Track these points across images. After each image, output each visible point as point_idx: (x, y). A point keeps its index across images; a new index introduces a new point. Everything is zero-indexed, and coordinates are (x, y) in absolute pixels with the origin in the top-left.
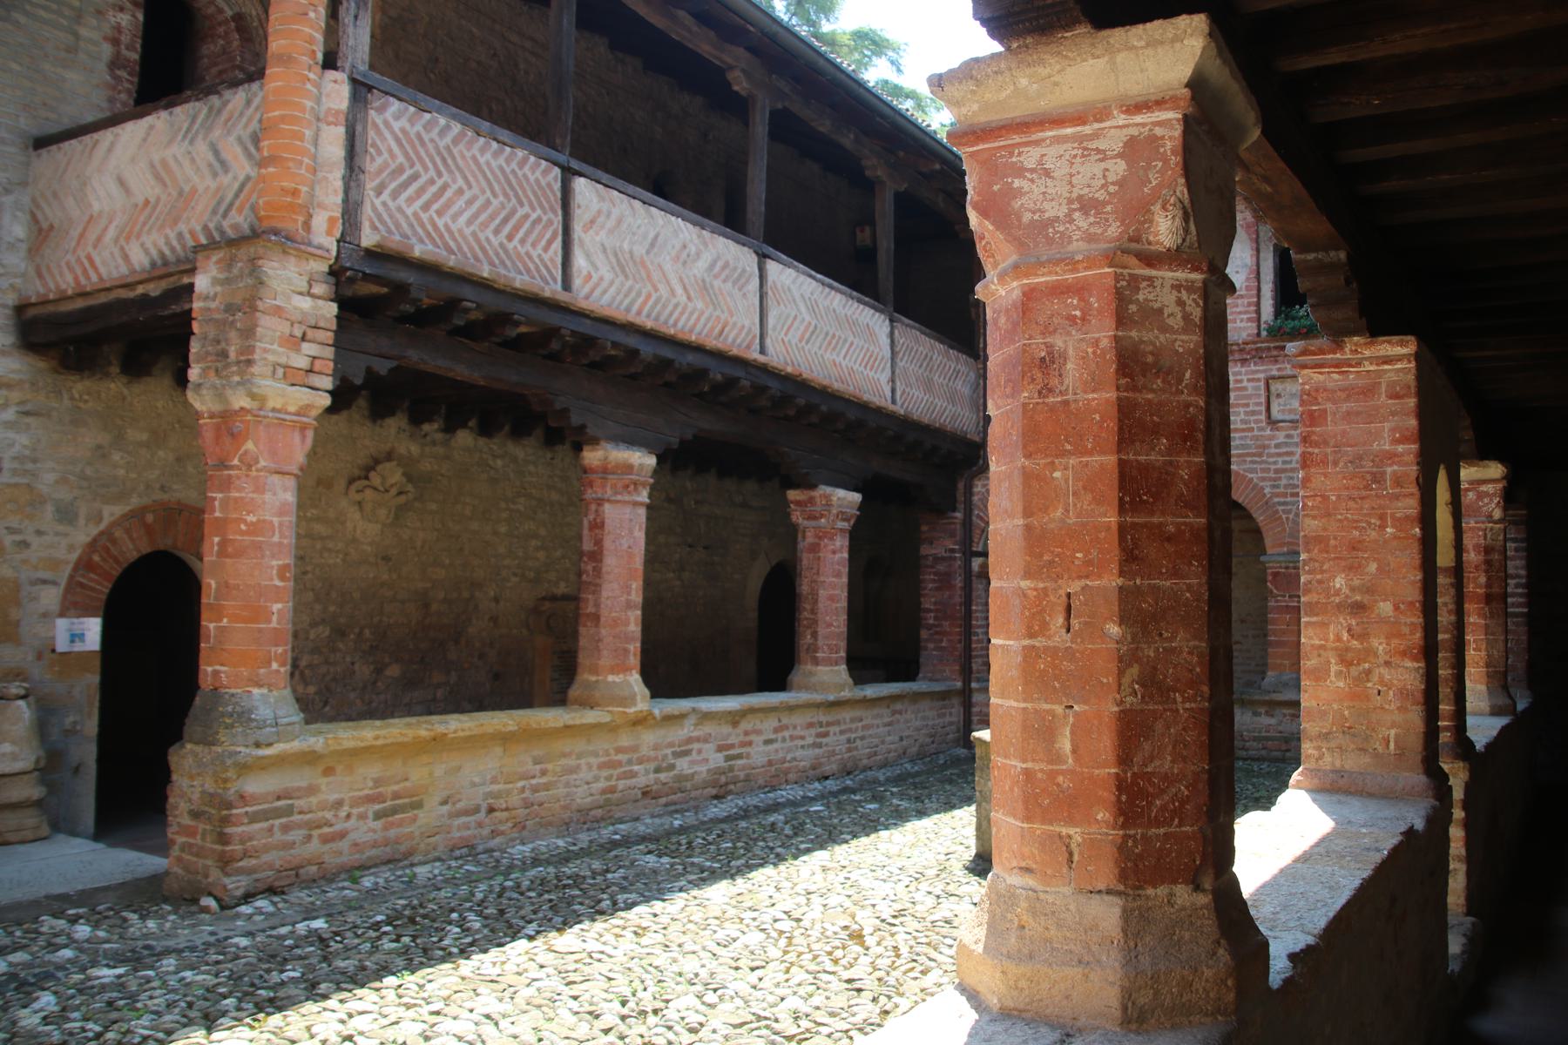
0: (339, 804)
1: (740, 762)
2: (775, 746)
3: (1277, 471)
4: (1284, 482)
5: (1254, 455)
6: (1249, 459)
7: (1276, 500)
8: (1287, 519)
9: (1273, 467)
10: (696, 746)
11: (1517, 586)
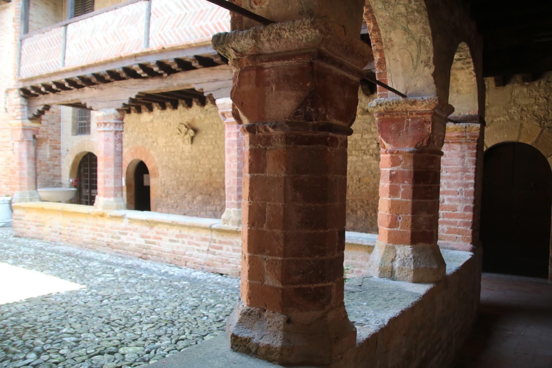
0: (28, 221)
1: (154, 246)
2: (177, 244)
10: (129, 232)
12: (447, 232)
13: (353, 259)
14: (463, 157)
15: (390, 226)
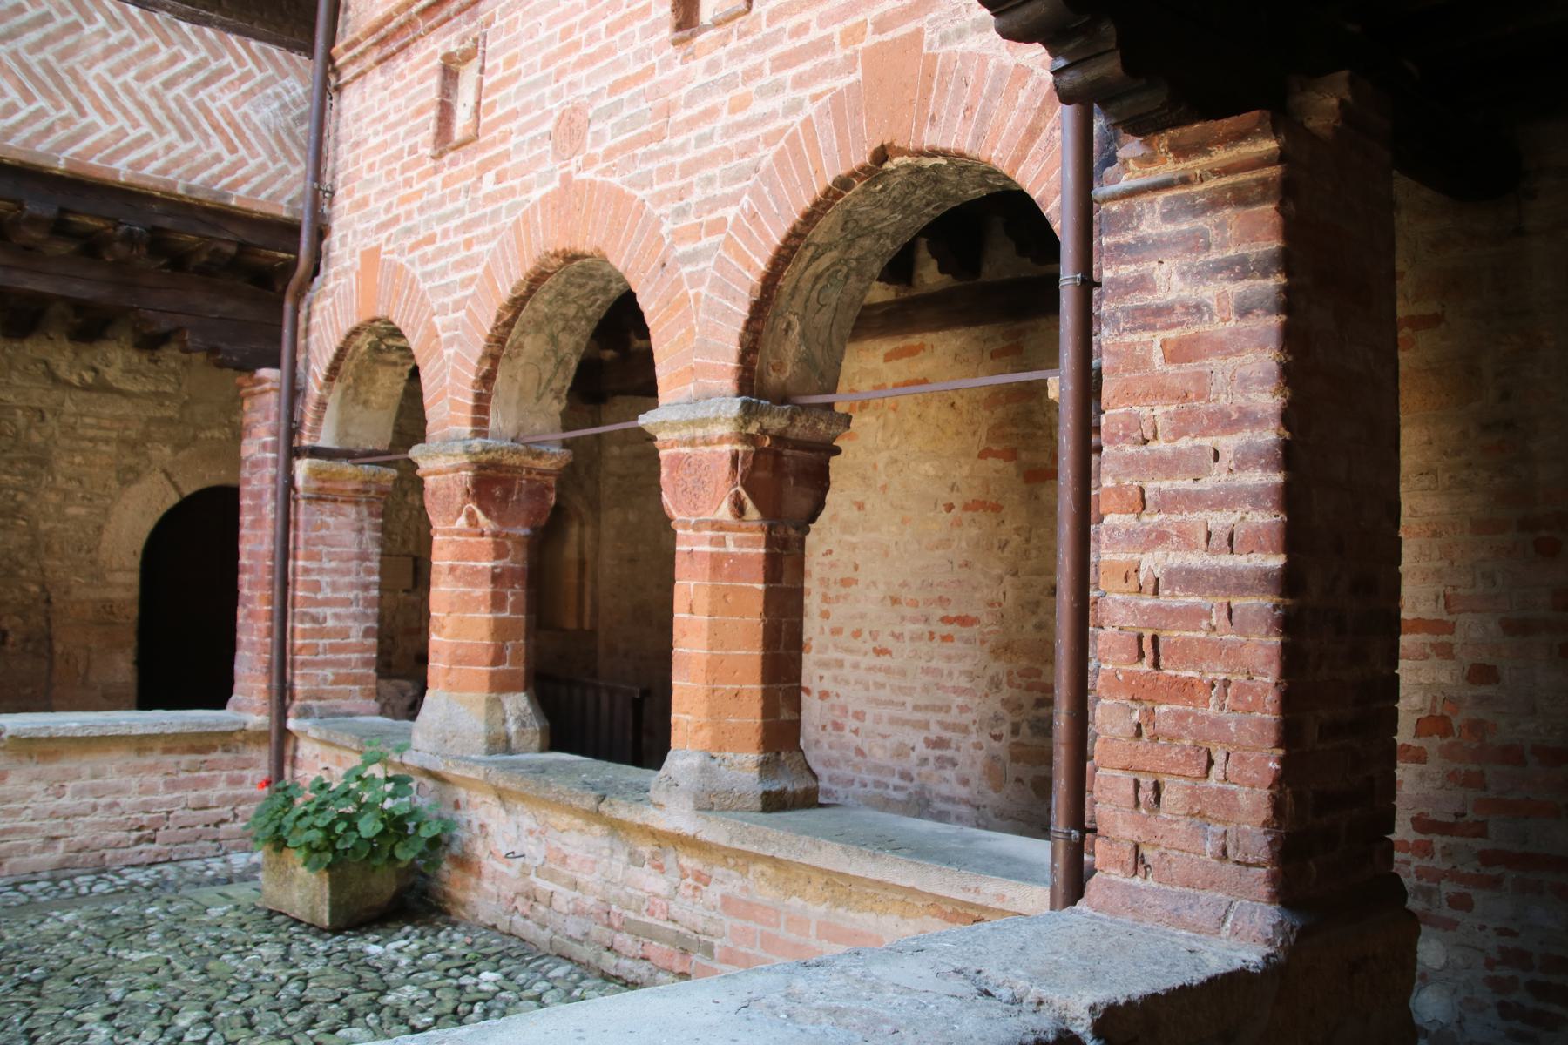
3: (688, 169)
4: (697, 195)
5: (650, 137)
6: (640, 151)
7: (680, 249)
8: (697, 297)
9: (679, 160)
11: (1244, 461)
12: (335, 683)
13: (95, 777)
14: (361, 531)
15: (494, 663)
